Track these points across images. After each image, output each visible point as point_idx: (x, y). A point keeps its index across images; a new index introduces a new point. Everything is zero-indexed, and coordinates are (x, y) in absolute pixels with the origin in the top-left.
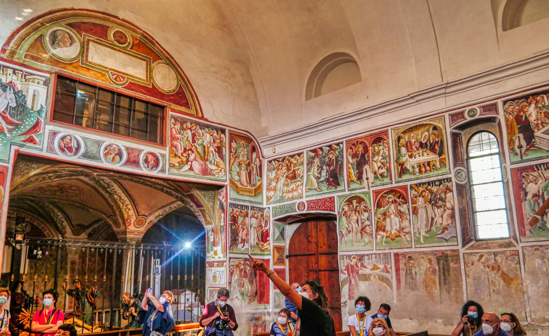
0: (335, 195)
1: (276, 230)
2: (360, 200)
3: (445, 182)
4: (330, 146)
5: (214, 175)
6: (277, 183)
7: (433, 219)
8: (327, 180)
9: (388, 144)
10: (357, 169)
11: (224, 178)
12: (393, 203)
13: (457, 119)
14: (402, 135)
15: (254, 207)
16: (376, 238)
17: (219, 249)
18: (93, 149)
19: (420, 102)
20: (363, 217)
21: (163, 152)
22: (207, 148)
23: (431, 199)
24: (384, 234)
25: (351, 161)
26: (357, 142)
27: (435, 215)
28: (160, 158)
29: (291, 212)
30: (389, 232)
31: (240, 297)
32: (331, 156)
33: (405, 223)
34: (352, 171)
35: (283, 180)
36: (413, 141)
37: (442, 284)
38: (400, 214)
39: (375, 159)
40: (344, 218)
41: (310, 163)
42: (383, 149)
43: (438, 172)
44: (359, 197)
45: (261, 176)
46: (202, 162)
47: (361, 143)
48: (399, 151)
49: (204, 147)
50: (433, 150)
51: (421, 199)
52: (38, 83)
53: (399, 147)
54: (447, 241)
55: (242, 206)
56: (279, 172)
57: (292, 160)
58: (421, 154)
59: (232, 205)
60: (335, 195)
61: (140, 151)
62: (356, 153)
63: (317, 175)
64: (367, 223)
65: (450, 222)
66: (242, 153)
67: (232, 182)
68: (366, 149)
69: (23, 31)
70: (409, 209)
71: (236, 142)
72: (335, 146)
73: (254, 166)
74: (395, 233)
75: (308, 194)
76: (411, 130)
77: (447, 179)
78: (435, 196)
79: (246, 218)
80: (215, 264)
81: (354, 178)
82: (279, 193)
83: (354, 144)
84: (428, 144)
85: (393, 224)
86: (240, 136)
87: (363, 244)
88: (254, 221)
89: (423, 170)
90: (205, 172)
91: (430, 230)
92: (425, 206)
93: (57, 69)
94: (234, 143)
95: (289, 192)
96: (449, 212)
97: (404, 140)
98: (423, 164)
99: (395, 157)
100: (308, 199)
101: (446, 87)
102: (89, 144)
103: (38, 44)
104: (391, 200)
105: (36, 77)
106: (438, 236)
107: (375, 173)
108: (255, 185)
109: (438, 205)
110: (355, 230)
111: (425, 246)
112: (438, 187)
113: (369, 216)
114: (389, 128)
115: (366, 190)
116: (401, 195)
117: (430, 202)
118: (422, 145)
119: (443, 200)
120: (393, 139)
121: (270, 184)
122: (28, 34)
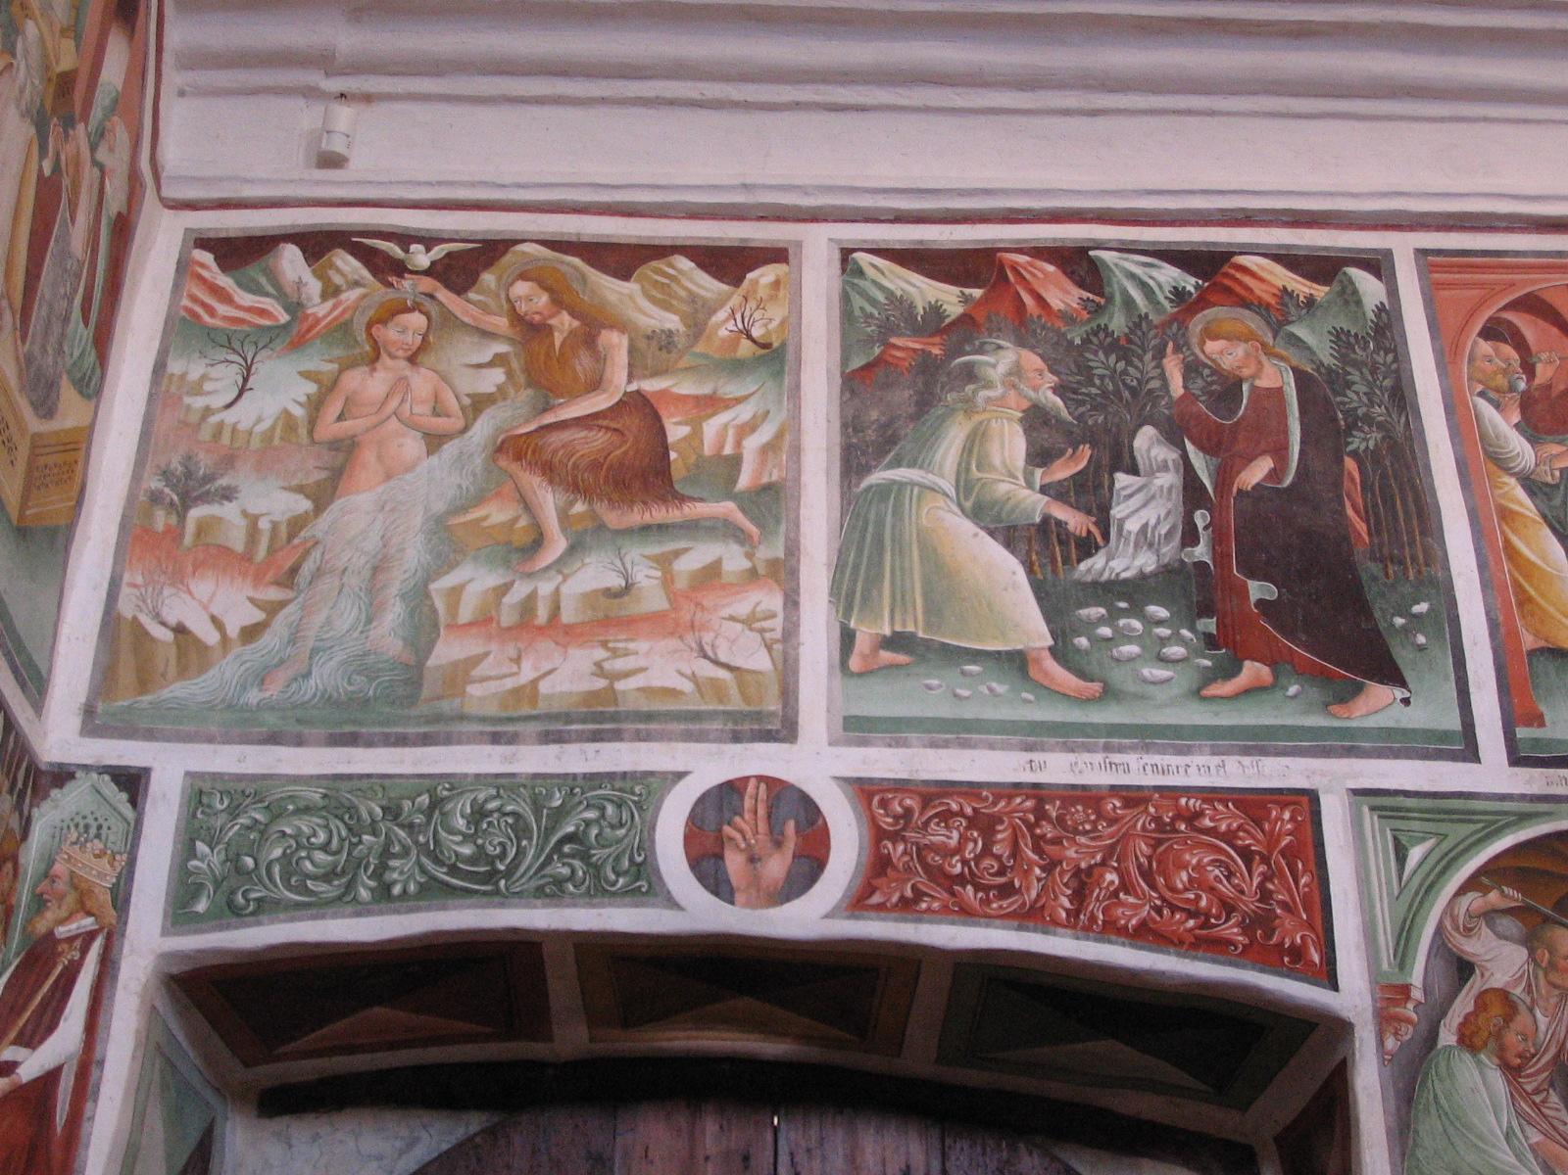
0: (1332, 779)
4: (1207, 263)
6: (322, 496)
8: (1194, 591)
29: (552, 892)
32: (1228, 355)
56: (371, 384)
60: (1332, 779)
63: (1034, 504)
72: (1282, 277)
75: (880, 701)
82: (347, 615)
95: (534, 626)
100: (884, 762)
121: (190, 488)
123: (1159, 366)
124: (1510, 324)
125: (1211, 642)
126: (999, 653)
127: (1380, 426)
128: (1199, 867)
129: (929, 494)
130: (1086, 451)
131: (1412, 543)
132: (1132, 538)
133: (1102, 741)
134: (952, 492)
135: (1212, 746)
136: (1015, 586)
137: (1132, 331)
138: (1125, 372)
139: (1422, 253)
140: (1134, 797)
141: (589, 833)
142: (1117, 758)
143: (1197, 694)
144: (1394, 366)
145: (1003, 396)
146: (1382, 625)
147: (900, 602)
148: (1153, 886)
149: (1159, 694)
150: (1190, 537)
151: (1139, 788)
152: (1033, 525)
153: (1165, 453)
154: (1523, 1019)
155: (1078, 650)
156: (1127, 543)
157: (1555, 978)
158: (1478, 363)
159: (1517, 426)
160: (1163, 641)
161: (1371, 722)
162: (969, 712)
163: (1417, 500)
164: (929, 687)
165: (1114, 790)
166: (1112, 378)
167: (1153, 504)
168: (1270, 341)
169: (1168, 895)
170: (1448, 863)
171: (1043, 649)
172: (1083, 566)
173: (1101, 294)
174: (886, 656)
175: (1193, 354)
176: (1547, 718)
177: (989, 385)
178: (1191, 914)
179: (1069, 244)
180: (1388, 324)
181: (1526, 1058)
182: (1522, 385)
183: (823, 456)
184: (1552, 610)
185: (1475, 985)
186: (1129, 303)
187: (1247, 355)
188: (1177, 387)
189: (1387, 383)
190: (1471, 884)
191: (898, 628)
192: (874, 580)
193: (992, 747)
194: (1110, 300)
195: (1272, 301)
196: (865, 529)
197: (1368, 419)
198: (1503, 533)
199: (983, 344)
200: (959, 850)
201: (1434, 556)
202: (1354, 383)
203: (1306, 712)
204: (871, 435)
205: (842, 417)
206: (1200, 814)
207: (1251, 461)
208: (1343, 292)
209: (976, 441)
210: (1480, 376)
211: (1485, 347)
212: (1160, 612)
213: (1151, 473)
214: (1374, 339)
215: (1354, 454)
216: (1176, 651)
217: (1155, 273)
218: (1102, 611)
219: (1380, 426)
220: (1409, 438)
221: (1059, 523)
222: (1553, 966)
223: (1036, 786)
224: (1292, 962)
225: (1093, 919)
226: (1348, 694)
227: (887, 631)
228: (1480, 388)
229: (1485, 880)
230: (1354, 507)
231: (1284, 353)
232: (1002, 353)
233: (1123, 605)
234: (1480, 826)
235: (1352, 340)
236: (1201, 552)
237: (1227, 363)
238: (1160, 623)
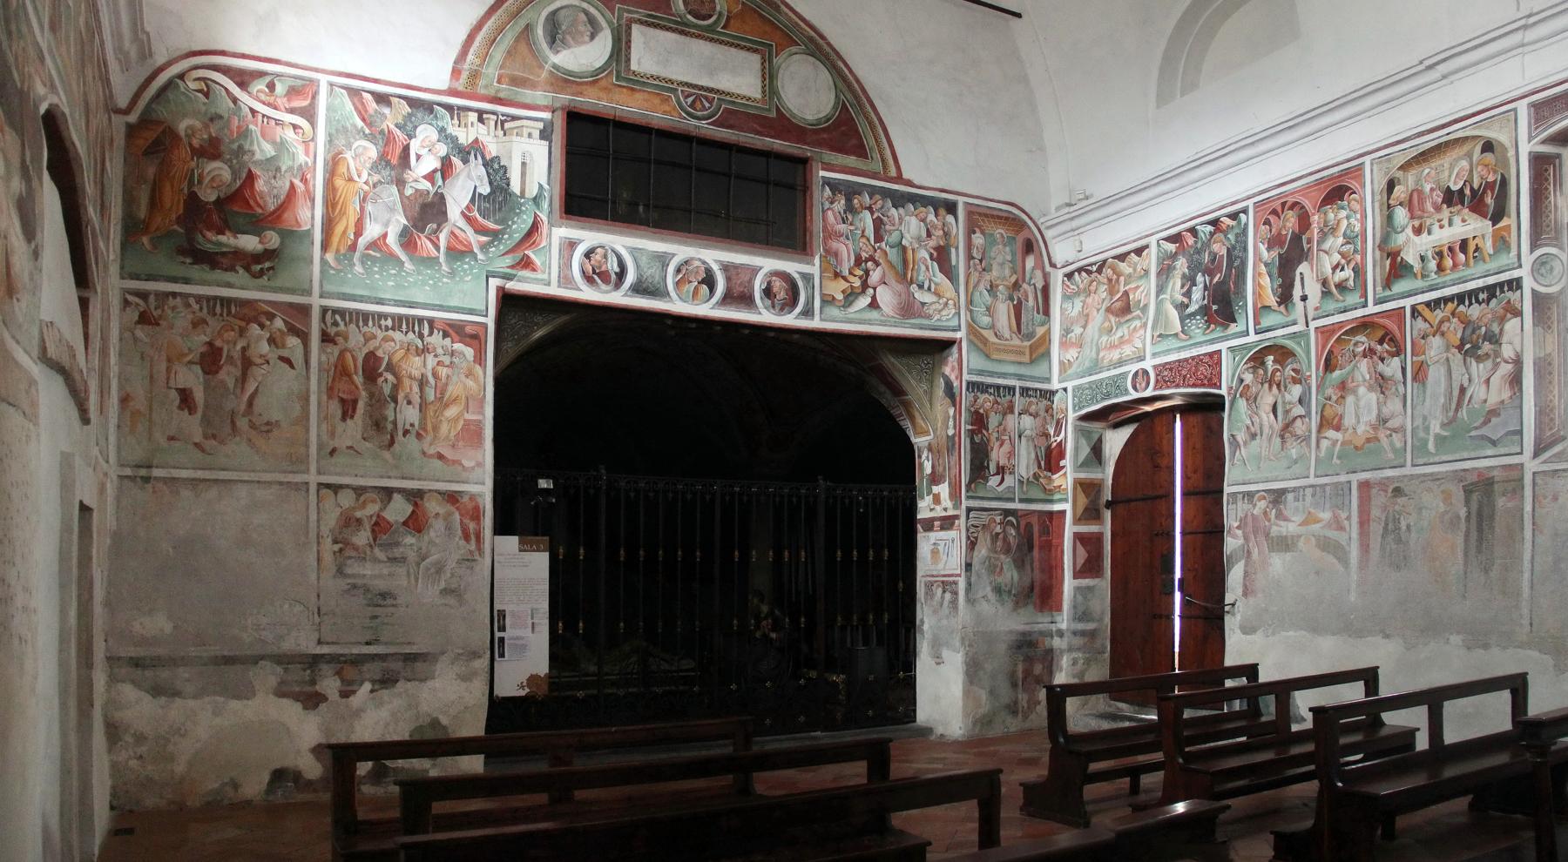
1: (1083, 442)
2: (1282, 353)
3: (1502, 292)
4: (1214, 222)
5: (929, 317)
6: (1084, 327)
7: (1463, 390)
8: (1204, 311)
9: (1362, 201)
11: (954, 323)
13: (1552, 115)
14: (1400, 174)
15: (1028, 389)
17: (943, 490)
18: (652, 272)
19: (1452, 78)
20: (1288, 397)
21: (806, 268)
22: (910, 252)
23: (1462, 339)
24: (1338, 436)
25: (1265, 254)
26: (1283, 204)
28: (800, 284)
31: (992, 596)
32: (1216, 247)
33: (1394, 405)
35: (1098, 319)
36: (1427, 188)
37: (1473, 551)
38: (1381, 383)
39: (1326, 246)
40: (1242, 404)
41: (1165, 271)
43: (1487, 267)
44: (1282, 347)
45: (1047, 312)
46: (899, 287)
48: (1389, 219)
49: (904, 249)
50: (1477, 207)
51: (1436, 342)
52: (530, 135)
53: (1389, 206)
55: (998, 387)
56: (1089, 300)
57: (1123, 266)
58: (1445, 222)
59: (972, 386)
60: (1223, 346)
61: (755, 271)
62: (1279, 234)
63: (1180, 298)
66: (1000, 259)
67: (973, 331)
68: (1304, 221)
69: (490, 23)
70: (1404, 370)
71: (983, 232)
73: (1030, 290)
75: (1159, 348)
76: (1424, 157)
77: (1510, 282)
78: (1473, 332)
79: (1009, 417)
80: (937, 523)
81: (1272, 300)
84: (1467, 192)
85: (1362, 408)
86: (993, 216)
87: (1285, 463)
88: (1027, 421)
89: (1448, 262)
90: (908, 309)
91: (1453, 420)
93: (565, 98)
94: (978, 234)
95: (1113, 347)
96: (1506, 369)
98: (1450, 249)
99: (1378, 235)
100: (1158, 361)
101: (1525, 27)
102: (644, 261)
103: (523, 47)
104: (1360, 349)
105: (525, 122)
106: (1473, 433)
107: (1325, 283)
108: (1030, 336)
110: (1266, 430)
111: (1437, 459)
113: (1304, 393)
114: (1367, 160)
116: (1386, 334)
117: (1460, 348)
118: (1451, 198)
119: (1494, 339)
122: (500, 30)
141: (1116, 384)
226: (1226, 327)
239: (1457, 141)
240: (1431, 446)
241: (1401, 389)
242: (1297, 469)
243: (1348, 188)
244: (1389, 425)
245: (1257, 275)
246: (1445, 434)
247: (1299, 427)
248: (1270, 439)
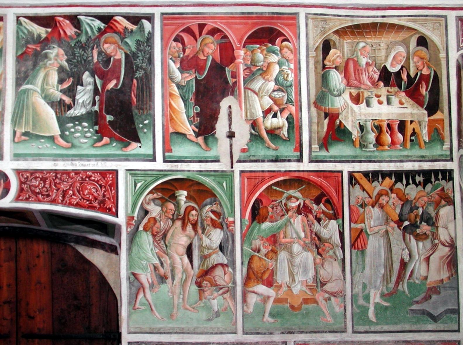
2: (200, 192)
4: (106, 19)
7: (404, 265)
8: (94, 118)
9: (296, 52)
10: (197, 102)
12: (299, 212)
16: (244, 300)
20: (206, 241)
23: (400, 215)
24: (271, 292)
26: (201, 27)
27: (410, 255)
30: (285, 288)
32: (108, 48)
33: (331, 269)
34: (179, 105)
36: (363, 61)
38: (318, 244)
39: (257, 84)
40: (146, 239)
42: (280, 64)
44: (199, 184)
47: (214, 32)
48: (324, 79)
50: (413, 93)
51: (376, 212)
53: (324, 67)
54: (435, 319)
58: (384, 99)
62: (195, 57)
63: (58, 95)
64: (220, 258)
65: (445, 275)
68: (227, 52)
74: (301, 291)
75: (22, 149)
78: (411, 210)
81: (189, 129)
83: (188, 31)
89: (387, 138)
92: (387, 232)
96: (443, 251)
97: (338, 53)
98: (389, 126)
99: (313, 92)
100: (23, 165)
104: (294, 204)
106: (415, 307)
107: (254, 125)
109: (418, 231)
111: (378, 328)
112: (420, 188)
115: (223, 166)
116: (322, 195)
117: (400, 222)
118: (386, 77)
120: (311, 42)
123: (92, 53)
124: (181, 36)
125: (97, 132)
126: (48, 136)
127: (144, 69)
128: (90, 189)
129: (35, 92)
130: (71, 79)
131: (147, 103)
132: (80, 104)
133: (71, 158)
134: (40, 91)
135: (95, 159)
136: (53, 118)
137: (87, 42)
138: (83, 55)
139: (162, 14)
140: (77, 172)
142: (74, 162)
143: (93, 146)
144: (150, 51)
145: (53, 63)
146: (137, 127)
147: (27, 123)
148: (80, 194)
149: (85, 146)
150: (94, 104)
151: (79, 170)
152: (57, 101)
153: (90, 80)
154: (158, 224)
155: (66, 135)
156: (79, 106)
157: (166, 214)
158: (172, 49)
159: (178, 68)
160: (86, 132)
161: (132, 152)
162: (41, 152)
163: (150, 92)
164: (33, 146)
165: (73, 171)
166: (80, 56)
167: (86, 94)
168: (120, 43)
169: (83, 196)
170: (146, 187)
171: (58, 135)
172: (68, 113)
173: (79, 30)
174: (24, 138)
175: (101, 49)
176: (173, 150)
177: (50, 60)
178: (88, 201)
179: (73, 14)
180: (150, 38)
181: (158, 233)
182: (182, 56)
183: (11, 81)
184: (179, 122)
185: (148, 216)
186: (87, 32)
187: (114, 48)
188: (95, 60)
189: (148, 56)
190: (151, 192)
191: (26, 130)
192: (21, 117)
193: (46, 160)
194: (82, 32)
195: (122, 31)
196: (20, 103)
197: (141, 67)
198: (169, 100)
199: (50, 46)
200: (38, 186)
201: (151, 108)
202: (139, 56)
203: (117, 150)
204: (22, 75)
205: (16, 69)
206: (91, 176)
207: (110, 81)
208: (140, 28)
209: (46, 76)
210: (171, 53)
211: (174, 44)
212: (85, 124)
213: (86, 86)
214: (146, 42)
215: (136, 78)
216: (89, 135)
217: (93, 22)
218: (72, 125)
219: (144, 69)
220: (151, 73)
221: (64, 101)
222: (166, 212)
223: (56, 170)
224: (109, 211)
225: (66, 202)
226: (127, 145)
227: (23, 131)
228: (171, 57)
229: (154, 191)
230: (134, 94)
231: (123, 47)
232: (55, 49)
233: (77, 123)
234: (154, 178)
235: (141, 43)
236: (96, 108)
237: (109, 51)
238: (85, 127)
239: (392, 26)
240: (371, 314)
241: (339, 252)
242: (218, 323)
243: (280, 34)
244: (327, 287)
245: (167, 95)
246: (386, 304)
247: (220, 276)
248: (183, 284)
